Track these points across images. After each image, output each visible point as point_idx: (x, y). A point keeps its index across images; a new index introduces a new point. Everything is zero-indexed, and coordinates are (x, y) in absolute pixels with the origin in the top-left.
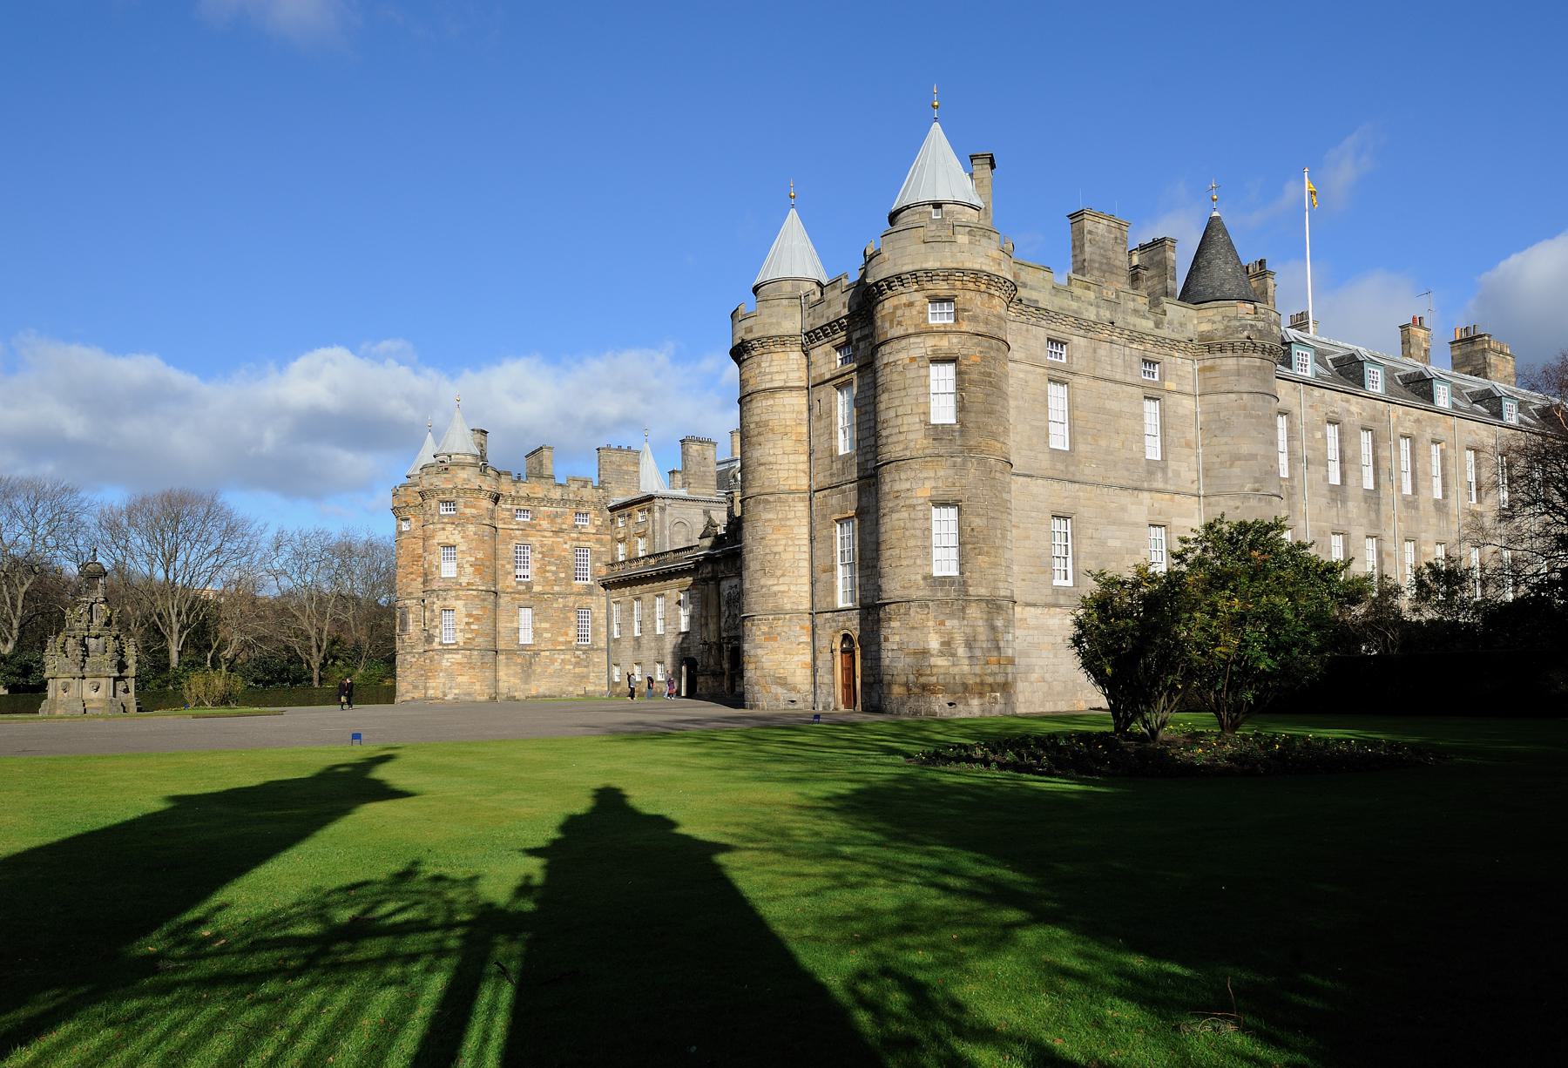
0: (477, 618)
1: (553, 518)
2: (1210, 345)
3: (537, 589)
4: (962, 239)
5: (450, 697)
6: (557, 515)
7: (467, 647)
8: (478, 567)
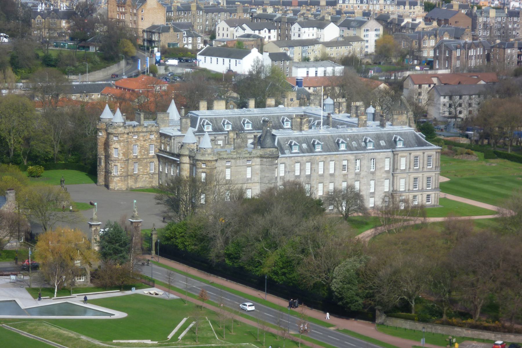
0: (123, 168)
1: (143, 137)
2: (261, 157)
3: (139, 157)
4: (207, 155)
5: (116, 189)
6: (145, 136)
7: (121, 176)
8: (124, 154)
